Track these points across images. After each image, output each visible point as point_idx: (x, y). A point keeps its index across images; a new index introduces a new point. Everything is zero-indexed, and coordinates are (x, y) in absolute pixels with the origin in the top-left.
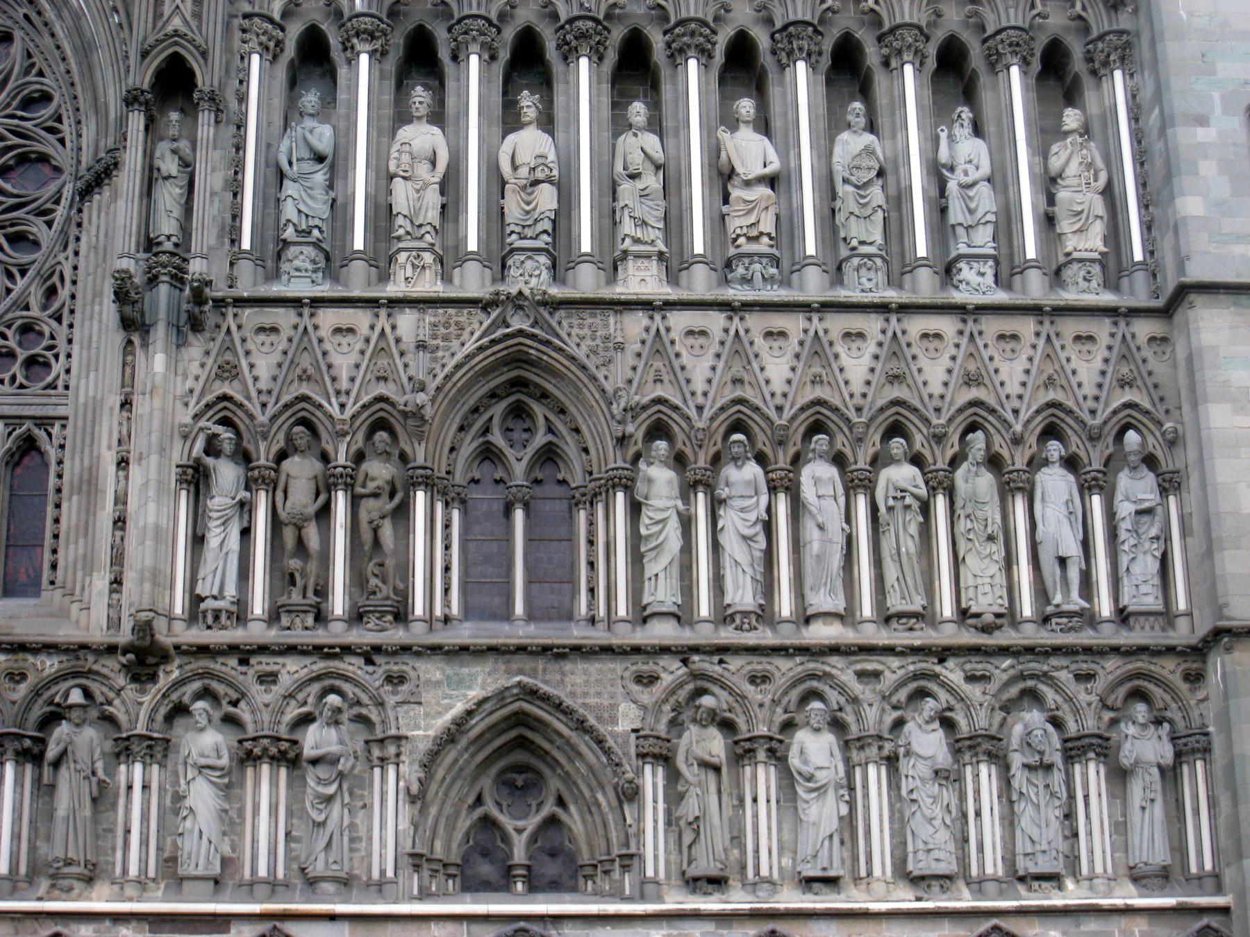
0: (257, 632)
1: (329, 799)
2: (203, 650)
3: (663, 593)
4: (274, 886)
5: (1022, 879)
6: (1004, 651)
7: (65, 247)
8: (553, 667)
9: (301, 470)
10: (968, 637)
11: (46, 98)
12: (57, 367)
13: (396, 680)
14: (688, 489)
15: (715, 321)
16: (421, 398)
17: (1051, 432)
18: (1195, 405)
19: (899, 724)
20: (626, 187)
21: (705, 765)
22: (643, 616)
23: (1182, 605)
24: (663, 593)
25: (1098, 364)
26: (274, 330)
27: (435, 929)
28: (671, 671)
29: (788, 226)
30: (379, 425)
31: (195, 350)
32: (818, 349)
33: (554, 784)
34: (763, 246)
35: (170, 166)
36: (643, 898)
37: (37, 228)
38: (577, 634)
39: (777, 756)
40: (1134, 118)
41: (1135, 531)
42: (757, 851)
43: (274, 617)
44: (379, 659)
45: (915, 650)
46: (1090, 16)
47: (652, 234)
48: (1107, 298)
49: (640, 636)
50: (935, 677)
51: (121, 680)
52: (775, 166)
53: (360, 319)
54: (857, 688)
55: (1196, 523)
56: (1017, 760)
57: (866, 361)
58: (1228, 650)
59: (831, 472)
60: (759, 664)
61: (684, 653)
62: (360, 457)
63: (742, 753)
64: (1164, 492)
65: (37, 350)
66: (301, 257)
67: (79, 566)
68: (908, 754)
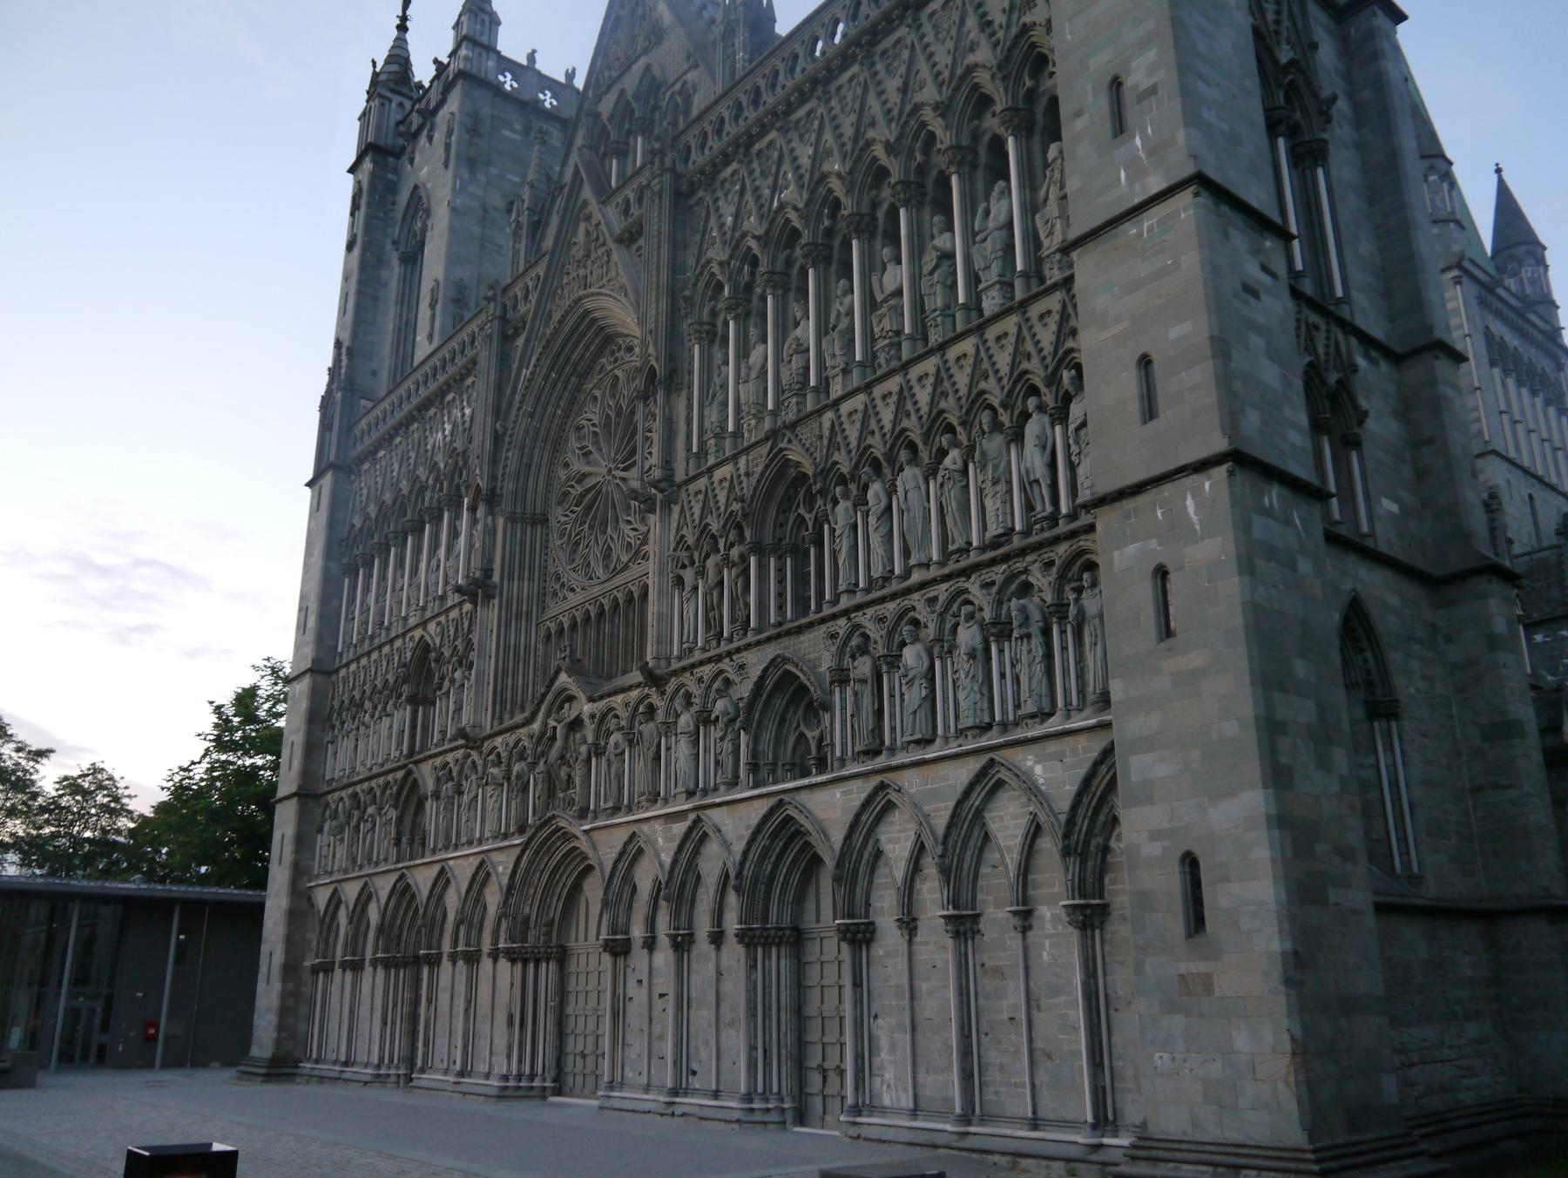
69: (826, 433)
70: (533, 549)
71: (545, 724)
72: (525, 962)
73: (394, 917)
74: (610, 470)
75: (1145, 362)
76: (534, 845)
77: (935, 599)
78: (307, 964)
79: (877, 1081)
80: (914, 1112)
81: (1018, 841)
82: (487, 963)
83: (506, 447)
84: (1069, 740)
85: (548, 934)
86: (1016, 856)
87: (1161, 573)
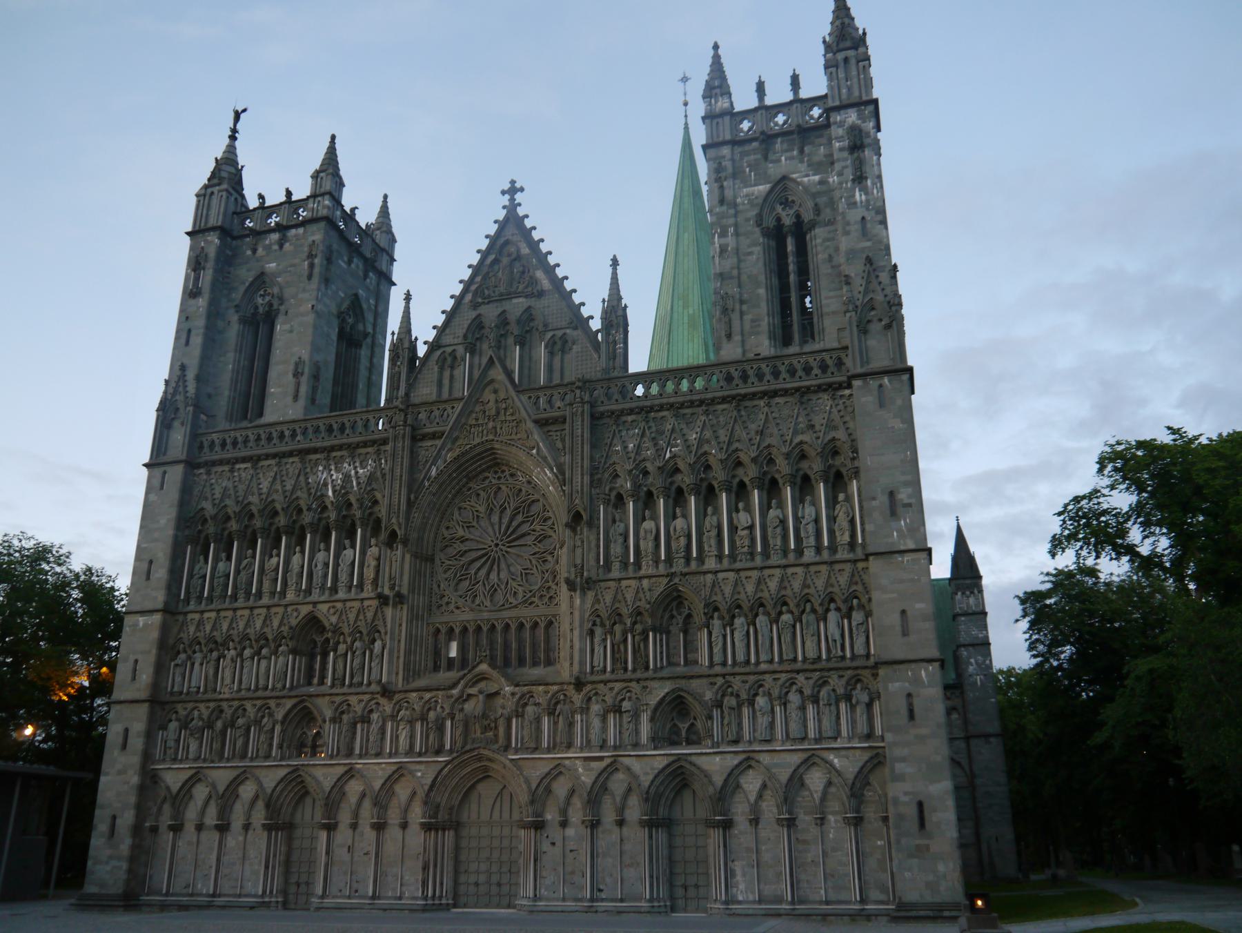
0: (608, 676)
2: (593, 682)
3: (717, 658)
4: (615, 748)
6: (815, 670)
9: (618, 628)
10: (807, 666)
12: (558, 599)
13: (645, 687)
15: (731, 575)
19: (787, 693)
21: (730, 708)
22: (712, 665)
23: (872, 652)
24: (717, 658)
27: (657, 758)
28: (720, 681)
29: (753, 540)
35: (579, 543)
36: (713, 747)
37: (549, 558)
38: (696, 670)
39: (751, 703)
41: (857, 629)
43: (613, 671)
45: (787, 672)
47: (713, 549)
48: (851, 556)
49: (712, 672)
56: (821, 703)
57: (775, 583)
60: (745, 678)
61: (724, 676)
62: (635, 623)
63: (740, 706)
64: (867, 618)
66: (616, 566)
69: (709, 585)
70: (425, 576)
71: (462, 691)
72: (437, 830)
73: (278, 797)
74: (497, 545)
75: (903, 612)
76: (456, 762)
77: (779, 679)
78: (147, 824)
79: (735, 890)
80: (760, 902)
81: (821, 787)
82: (393, 833)
83: (414, 510)
84: (852, 751)
85: (450, 814)
86: (819, 794)
87: (909, 695)
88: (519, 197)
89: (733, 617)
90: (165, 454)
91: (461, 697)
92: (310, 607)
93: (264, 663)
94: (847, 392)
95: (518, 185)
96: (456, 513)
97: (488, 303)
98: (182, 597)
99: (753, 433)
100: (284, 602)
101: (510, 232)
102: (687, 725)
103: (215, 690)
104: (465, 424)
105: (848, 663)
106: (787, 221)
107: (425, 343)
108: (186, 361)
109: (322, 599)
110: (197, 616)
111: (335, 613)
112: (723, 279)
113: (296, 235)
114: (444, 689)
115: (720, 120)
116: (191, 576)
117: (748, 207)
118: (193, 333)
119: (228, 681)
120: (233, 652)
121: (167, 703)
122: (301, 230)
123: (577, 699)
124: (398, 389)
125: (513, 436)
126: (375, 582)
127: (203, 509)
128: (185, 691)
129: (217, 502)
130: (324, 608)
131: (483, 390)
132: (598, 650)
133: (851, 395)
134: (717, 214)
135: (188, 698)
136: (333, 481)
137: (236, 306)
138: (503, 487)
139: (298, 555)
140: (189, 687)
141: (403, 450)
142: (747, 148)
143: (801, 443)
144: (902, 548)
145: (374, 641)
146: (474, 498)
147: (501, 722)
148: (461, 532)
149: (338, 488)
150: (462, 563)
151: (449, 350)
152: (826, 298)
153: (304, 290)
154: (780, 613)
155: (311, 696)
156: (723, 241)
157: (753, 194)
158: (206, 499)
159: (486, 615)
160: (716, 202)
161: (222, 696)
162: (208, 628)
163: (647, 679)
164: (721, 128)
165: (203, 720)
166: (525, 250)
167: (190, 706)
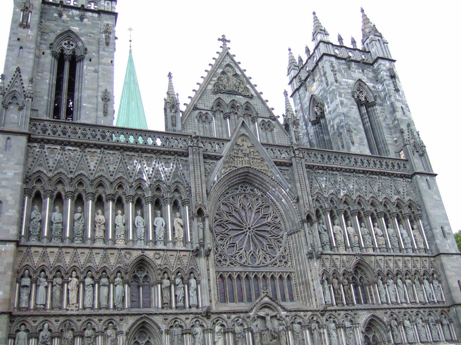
0: (335, 307)
1: (351, 334)
2: (331, 310)
5: (434, 342)
6: (428, 308)
7: (286, 243)
8: (375, 311)
11: (276, 218)
12: (289, 263)
13: (355, 314)
14: (383, 283)
15: (382, 258)
16: (351, 270)
17: (424, 274)
18: (443, 270)
20: (365, 236)
23: (445, 300)
24: (384, 300)
25: (428, 264)
26: (328, 259)
28: (389, 312)
29: (386, 244)
30: (344, 274)
31: (319, 261)
32: (396, 262)
33: (373, 330)
34: (384, 246)
35: (310, 232)
38: (376, 306)
40: (424, 227)
42: (404, 339)
44: (353, 311)
45: (417, 308)
46: (415, 211)
47: (371, 244)
50: (419, 312)
51: (320, 316)
52: (382, 234)
53: (339, 257)
54: (411, 313)
55: (444, 288)
56: (431, 324)
58: (456, 307)
59: (400, 281)
60: (399, 310)
61: (389, 309)
63: (399, 324)
65: (286, 260)
67: (307, 297)
68: (419, 323)
74: (249, 228)
88: (228, 45)
89: (387, 280)
90: (4, 125)
91: (254, 318)
92: (140, 253)
93: (105, 290)
94: (409, 180)
95: (227, 39)
96: (222, 206)
97: (224, 93)
98: (23, 234)
99: (377, 191)
100: (116, 246)
101: (228, 61)
102: (372, 336)
103: (61, 308)
104: (231, 155)
105: (437, 305)
106: (363, 99)
107: (185, 104)
108: (22, 68)
109: (147, 247)
110: (40, 250)
111: (159, 258)
112: (344, 116)
113: (92, 17)
114: (247, 312)
115: (327, 45)
116: (30, 220)
117: (347, 87)
118: (25, 50)
119: (73, 299)
120: (75, 280)
121: (19, 316)
122: (96, 15)
123: (323, 320)
124: (175, 126)
125: (260, 168)
126: (185, 241)
127: (39, 171)
128: (32, 307)
129: (53, 169)
130: (150, 254)
131: (239, 138)
132: (327, 292)
133: (411, 181)
134: (335, 86)
135: (36, 313)
136: (147, 171)
137: (52, 44)
138: (248, 196)
139: (119, 217)
140: (36, 304)
141: (200, 162)
142: (340, 61)
143: (398, 199)
144: (452, 252)
145: (189, 279)
146: (231, 198)
147: (283, 333)
148: (226, 218)
149: (150, 176)
150: (230, 236)
151: (204, 112)
152: (387, 137)
153: (104, 50)
154: (406, 279)
155: (151, 314)
156: (341, 99)
157: (348, 82)
158: (41, 165)
159: (250, 269)
160: (334, 80)
161: (69, 312)
162: (52, 259)
163: (357, 309)
164: (328, 49)
165: (50, 330)
166: (239, 73)
167: (41, 319)
